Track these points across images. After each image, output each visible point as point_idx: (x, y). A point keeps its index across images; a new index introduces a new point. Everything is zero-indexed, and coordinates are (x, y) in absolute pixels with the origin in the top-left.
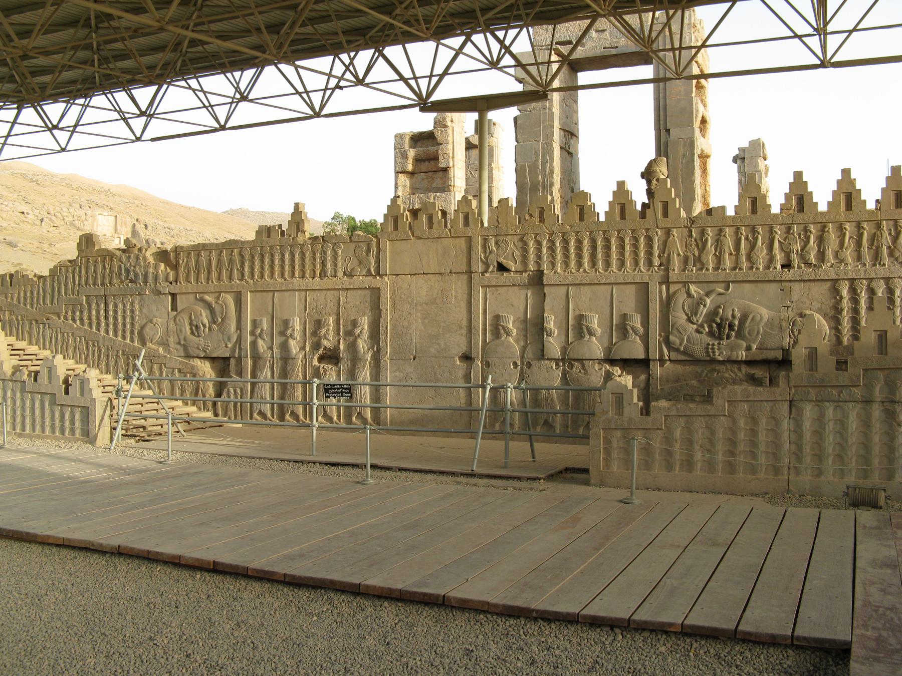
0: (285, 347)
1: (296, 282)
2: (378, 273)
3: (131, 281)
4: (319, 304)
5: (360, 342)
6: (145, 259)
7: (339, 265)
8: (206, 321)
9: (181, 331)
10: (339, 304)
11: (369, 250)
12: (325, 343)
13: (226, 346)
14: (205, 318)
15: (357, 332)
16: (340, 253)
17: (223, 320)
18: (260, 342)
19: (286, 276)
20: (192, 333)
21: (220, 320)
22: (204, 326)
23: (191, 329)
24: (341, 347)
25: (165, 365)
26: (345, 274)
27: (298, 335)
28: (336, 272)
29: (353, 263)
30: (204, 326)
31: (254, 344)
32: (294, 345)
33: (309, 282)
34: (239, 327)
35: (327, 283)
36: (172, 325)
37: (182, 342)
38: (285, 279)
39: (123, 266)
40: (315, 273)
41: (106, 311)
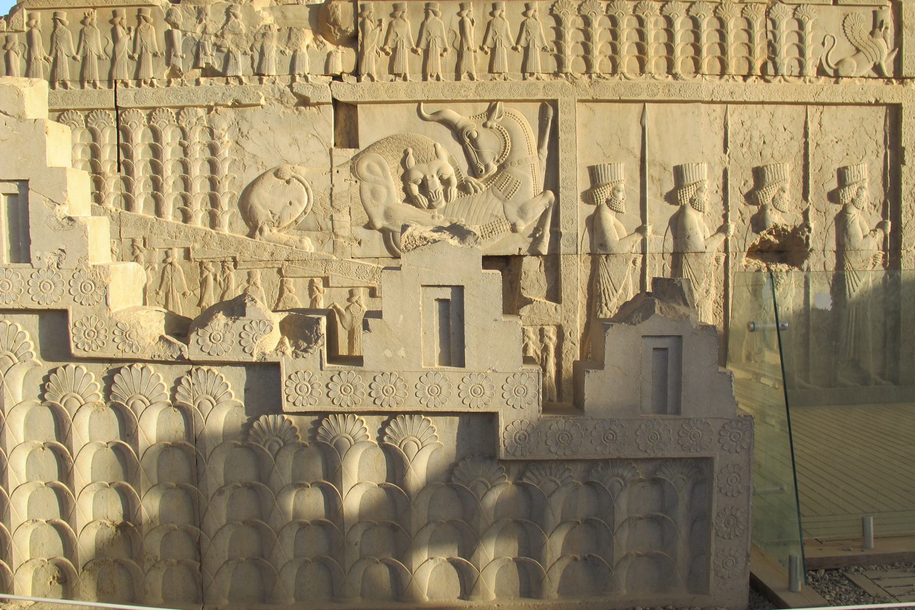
0: (678, 225)
1: (709, 84)
2: (899, 75)
3: (209, 72)
4: (756, 134)
5: (855, 214)
6: (252, 17)
7: (809, 53)
8: (450, 172)
9: (374, 193)
10: (806, 135)
11: (877, 24)
12: (775, 218)
13: (514, 229)
14: (448, 159)
15: (849, 194)
16: (809, 26)
17: (502, 167)
18: (609, 217)
19: (678, 69)
20: (410, 199)
21: (494, 168)
22: (446, 183)
23: (407, 189)
24: (812, 225)
25: (326, 282)
26: (821, 72)
27: (709, 197)
28: (801, 65)
29: (843, 49)
30: (446, 183)
31: (594, 224)
32: (700, 225)
33: (734, 87)
34: (552, 182)
35: (776, 89)
36: (343, 182)
37: (379, 223)
38: (675, 76)
39: (177, 34)
40: (751, 67)
41: (124, 148)
